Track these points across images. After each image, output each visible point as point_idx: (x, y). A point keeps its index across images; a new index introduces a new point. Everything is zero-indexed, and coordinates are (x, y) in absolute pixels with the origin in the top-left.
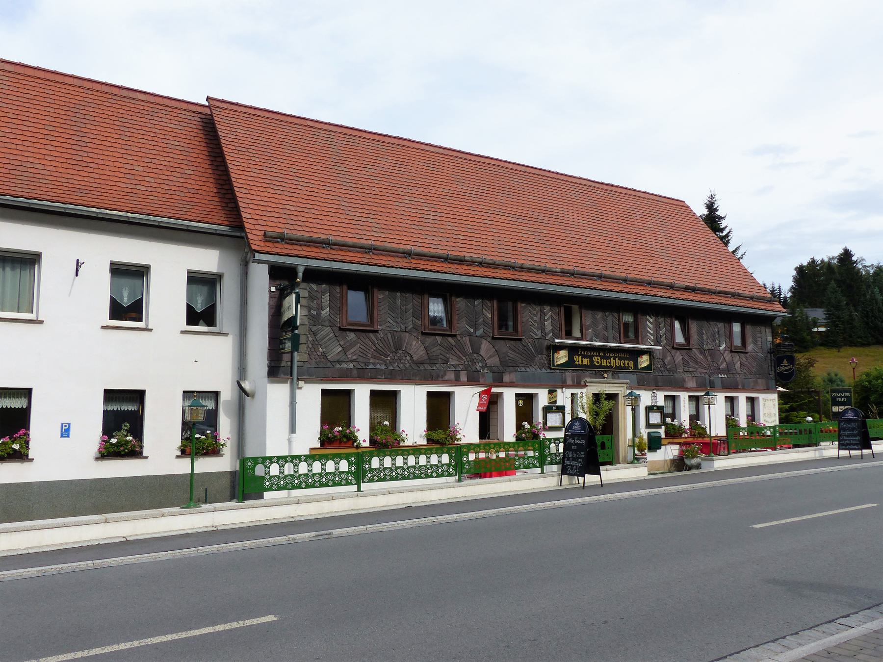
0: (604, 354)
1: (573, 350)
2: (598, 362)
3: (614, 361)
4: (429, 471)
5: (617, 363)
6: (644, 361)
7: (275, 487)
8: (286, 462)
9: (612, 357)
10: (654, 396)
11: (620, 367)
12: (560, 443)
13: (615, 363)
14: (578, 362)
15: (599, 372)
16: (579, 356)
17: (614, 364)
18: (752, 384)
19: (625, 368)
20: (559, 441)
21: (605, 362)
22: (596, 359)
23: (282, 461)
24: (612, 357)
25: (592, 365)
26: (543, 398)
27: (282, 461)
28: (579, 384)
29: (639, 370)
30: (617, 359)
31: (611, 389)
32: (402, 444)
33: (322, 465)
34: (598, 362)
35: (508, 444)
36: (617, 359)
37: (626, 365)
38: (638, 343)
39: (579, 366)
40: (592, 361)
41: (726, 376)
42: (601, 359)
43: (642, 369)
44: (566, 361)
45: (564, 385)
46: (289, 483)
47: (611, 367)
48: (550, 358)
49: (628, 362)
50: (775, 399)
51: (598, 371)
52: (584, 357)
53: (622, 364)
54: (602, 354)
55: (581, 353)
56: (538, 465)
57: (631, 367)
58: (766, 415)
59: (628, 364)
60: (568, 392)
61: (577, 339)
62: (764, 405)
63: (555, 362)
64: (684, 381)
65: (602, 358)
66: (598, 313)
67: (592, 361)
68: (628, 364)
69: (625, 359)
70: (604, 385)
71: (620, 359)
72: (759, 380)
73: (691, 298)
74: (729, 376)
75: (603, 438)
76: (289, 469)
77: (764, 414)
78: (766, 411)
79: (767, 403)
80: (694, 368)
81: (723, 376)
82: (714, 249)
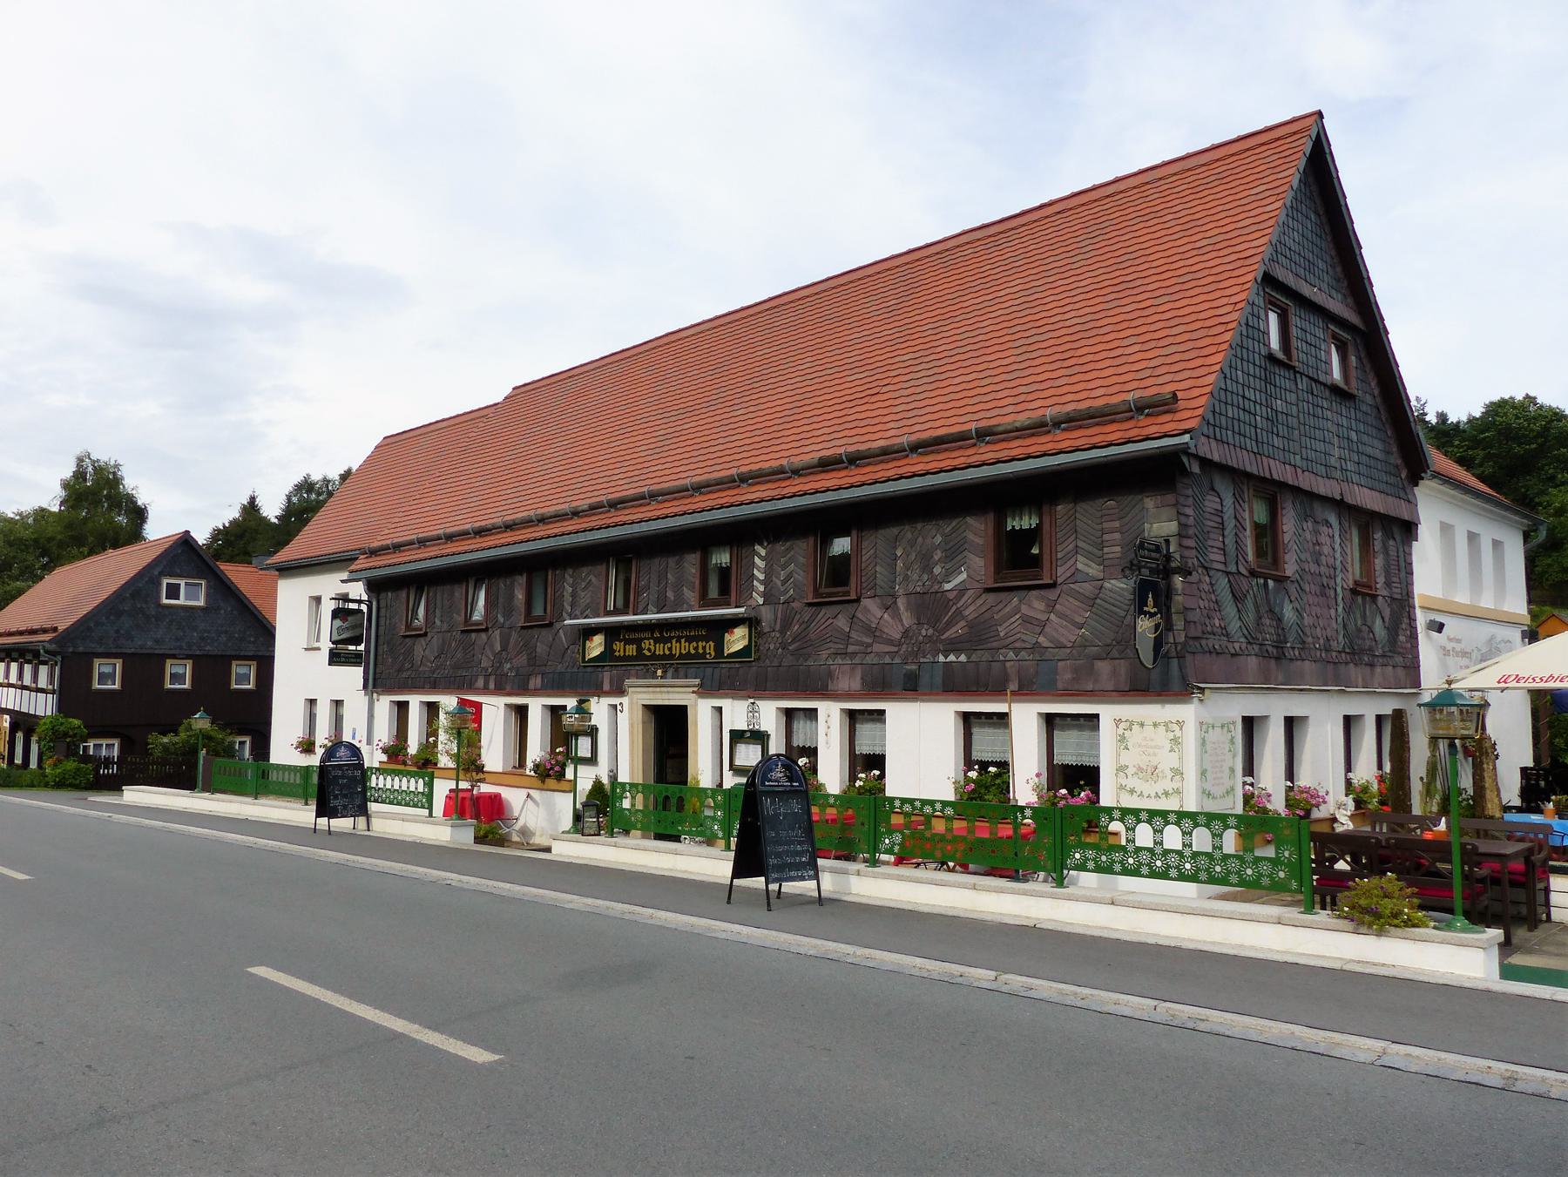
0: (661, 633)
1: (612, 632)
2: (649, 650)
3: (678, 644)
4: (1131, 861)
5: (683, 648)
6: (737, 640)
7: (1173, 873)
8: (1196, 825)
9: (673, 637)
10: (753, 710)
11: (688, 656)
12: (1227, 827)
13: (680, 647)
14: (619, 651)
15: (645, 666)
16: (620, 642)
17: (678, 650)
18: (1068, 676)
19: (697, 656)
20: (933, 807)
21: (661, 648)
22: (646, 644)
23: (1158, 821)
24: (673, 637)
25: (640, 655)
26: (701, 713)
27: (1158, 821)
28: (620, 692)
29: (727, 657)
30: (683, 640)
31: (671, 696)
32: (1316, 814)
33: (1221, 846)
34: (649, 650)
35: (705, 790)
36: (683, 640)
37: (701, 651)
38: (727, 605)
39: (620, 659)
40: (640, 649)
41: (963, 658)
42: (655, 644)
43: (732, 655)
44: (745, 647)
45: (600, 692)
46: (1158, 866)
47: (671, 656)
48: (755, 646)
49: (704, 643)
50: (1234, 723)
51: (652, 664)
52: (628, 642)
53: (691, 648)
54: (657, 635)
55: (624, 636)
56: (426, 806)
57: (710, 653)
58: (1131, 771)
59: (704, 648)
60: (606, 701)
61: (616, 612)
62: (1122, 739)
63: (587, 655)
64: (830, 675)
65: (657, 641)
66: (583, 569)
67: (640, 649)
68: (704, 648)
69: (697, 639)
70: (658, 689)
71: (689, 640)
72: (1099, 665)
73: (556, 531)
74: (973, 657)
75: (667, 788)
76: (1173, 838)
77: (1121, 769)
78: (1131, 758)
79: (1135, 736)
80: (861, 643)
81: (952, 658)
82: (587, 436)
